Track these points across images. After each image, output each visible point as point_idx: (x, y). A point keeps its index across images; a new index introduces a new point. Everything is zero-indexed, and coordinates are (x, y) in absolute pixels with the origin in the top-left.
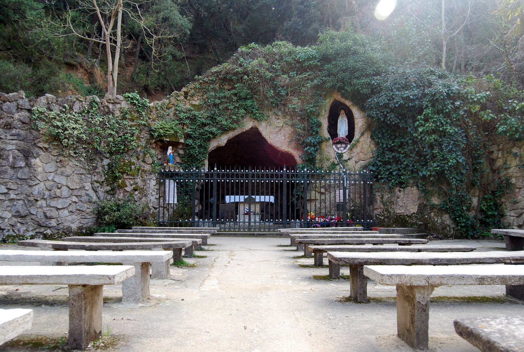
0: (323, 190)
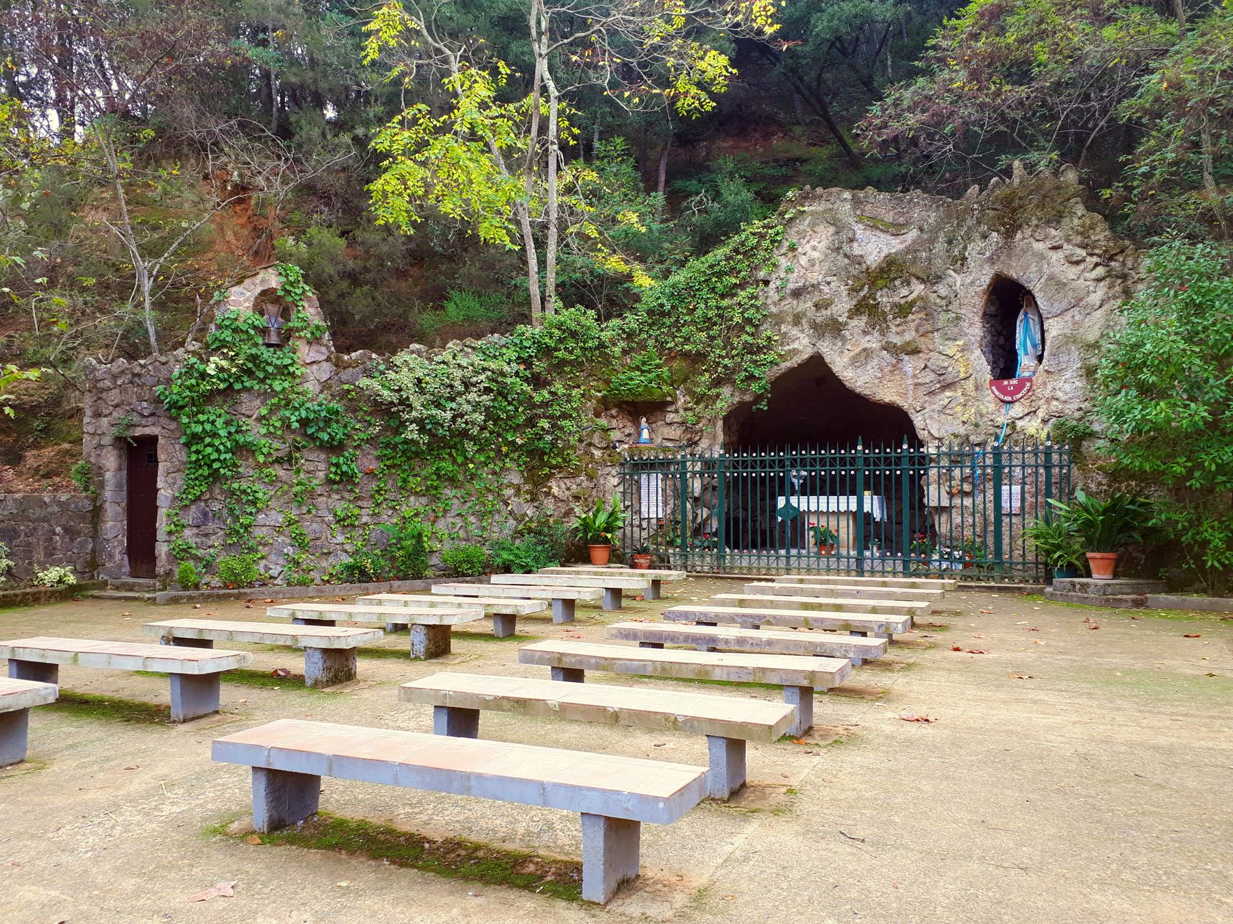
0: (967, 487)
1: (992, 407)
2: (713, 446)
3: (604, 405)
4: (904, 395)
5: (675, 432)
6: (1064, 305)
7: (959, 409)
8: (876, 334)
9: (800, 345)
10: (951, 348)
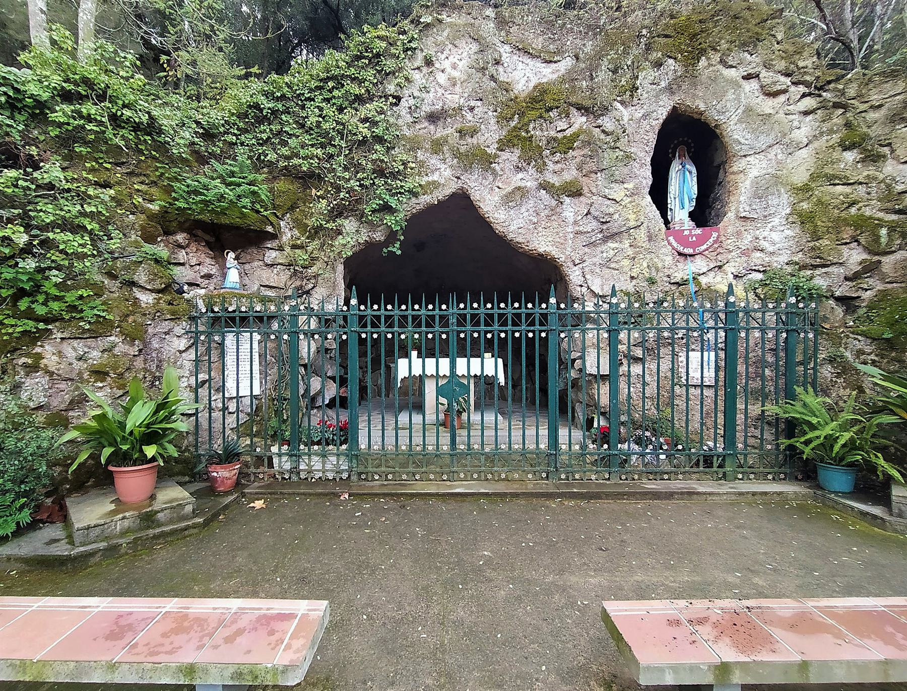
0: (639, 352)
1: (669, 260)
2: (330, 294)
3: (164, 225)
4: (561, 245)
5: (279, 277)
6: (770, 140)
7: (626, 262)
8: (532, 171)
9: (441, 177)
10: (618, 192)
